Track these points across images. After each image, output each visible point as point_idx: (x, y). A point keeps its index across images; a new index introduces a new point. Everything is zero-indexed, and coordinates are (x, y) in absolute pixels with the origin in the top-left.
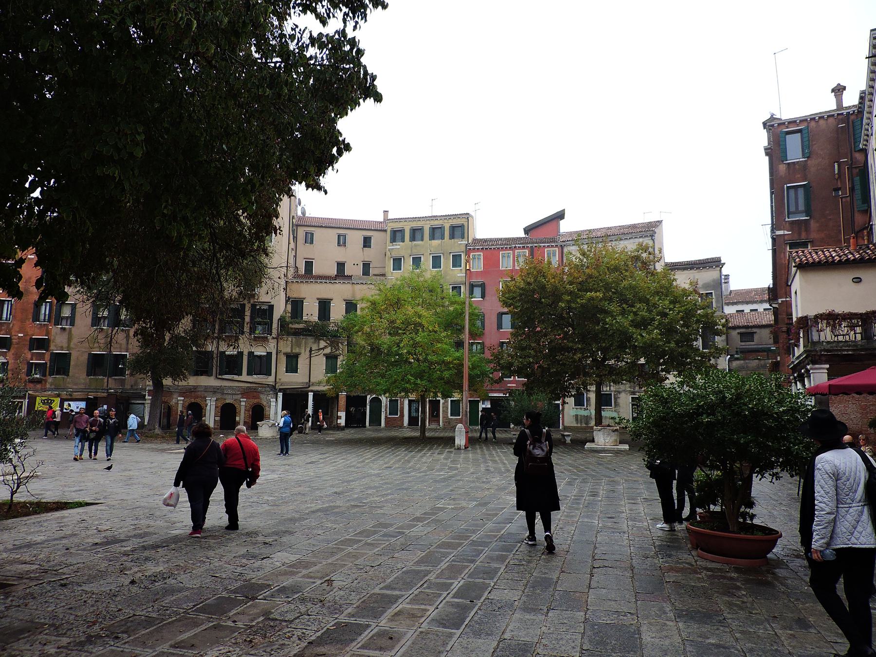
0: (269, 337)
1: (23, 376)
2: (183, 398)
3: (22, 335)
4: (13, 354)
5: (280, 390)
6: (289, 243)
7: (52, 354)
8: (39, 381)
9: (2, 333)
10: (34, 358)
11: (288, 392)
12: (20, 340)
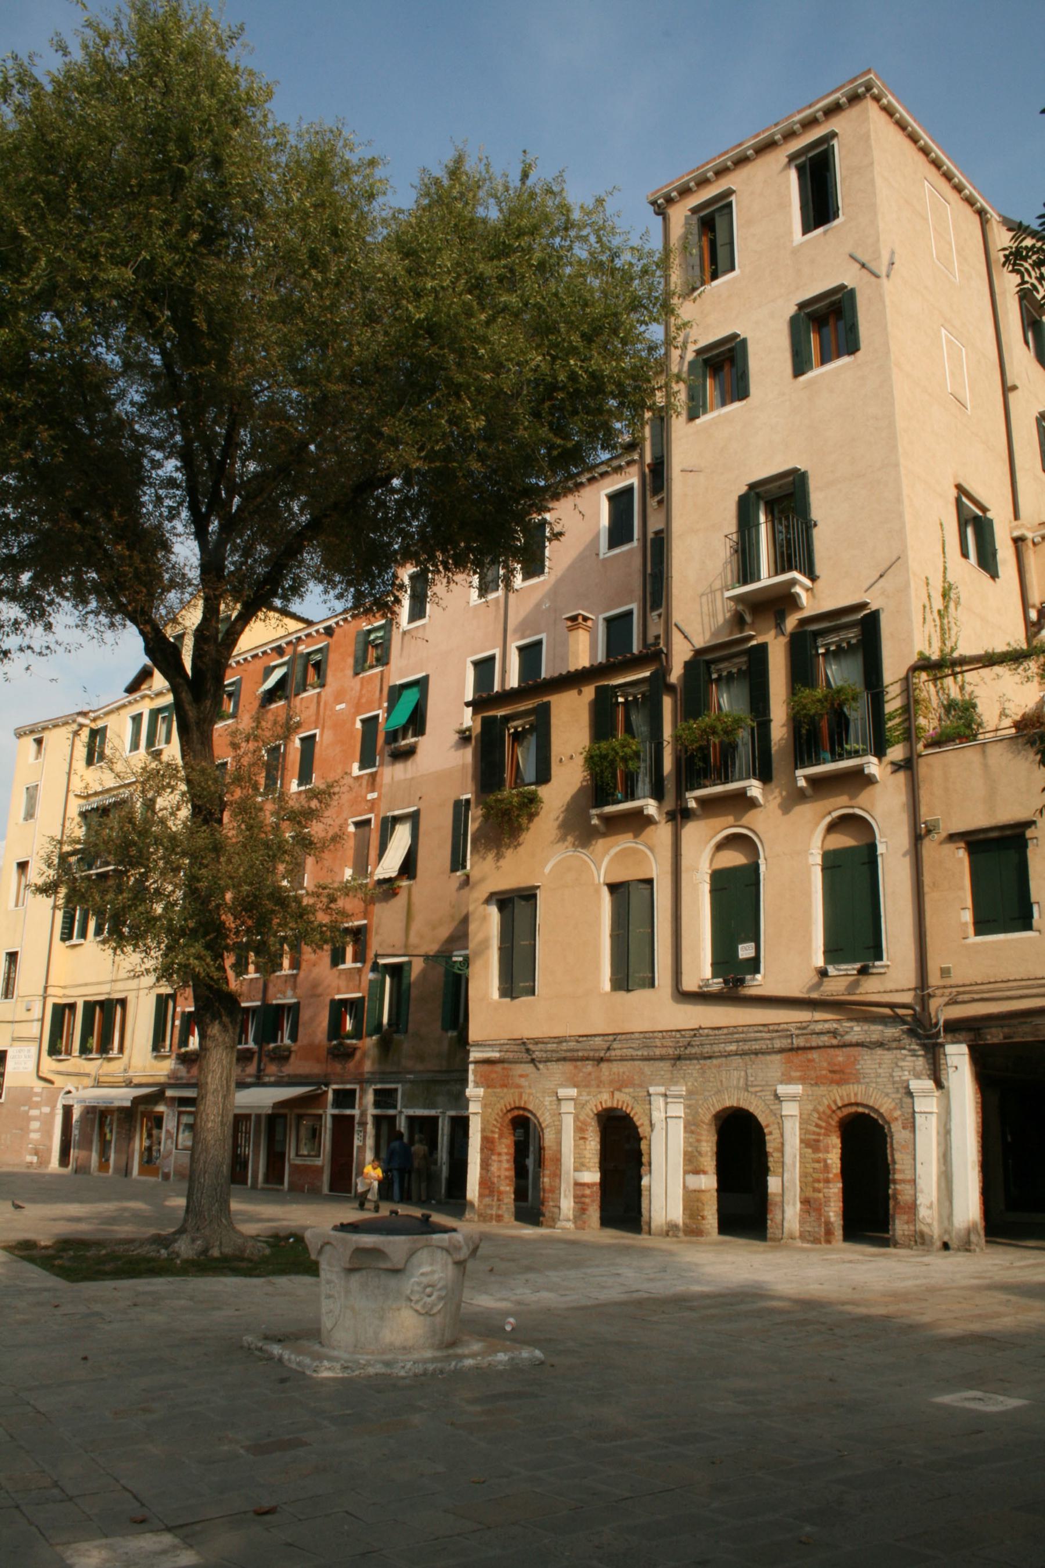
0: (873, 766)
2: (573, 1092)
5: (955, 1028)
6: (1007, 390)
11: (994, 1036)
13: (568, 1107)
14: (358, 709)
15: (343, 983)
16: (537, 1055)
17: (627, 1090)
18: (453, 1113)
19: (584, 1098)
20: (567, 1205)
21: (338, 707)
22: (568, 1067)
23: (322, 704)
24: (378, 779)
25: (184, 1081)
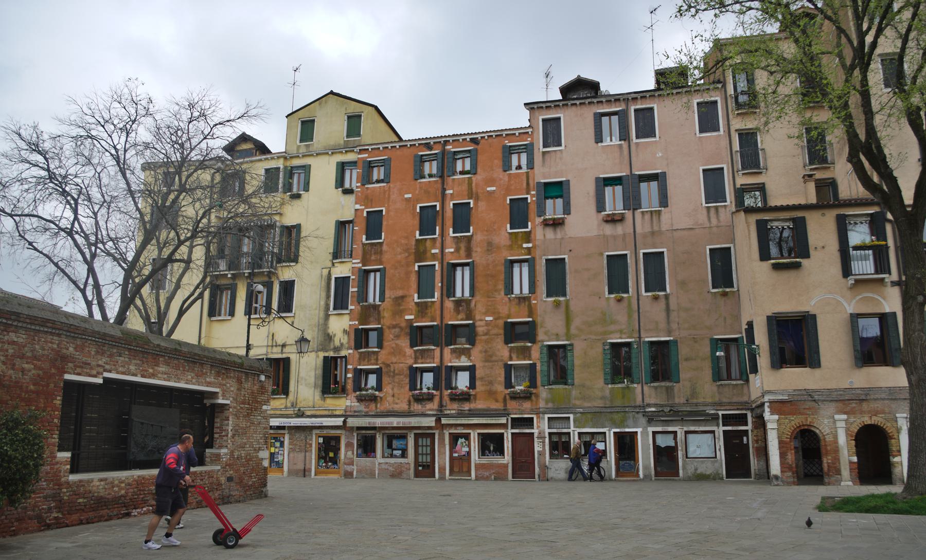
1: (500, 388)
2: (845, 417)
3: (491, 318)
4: (481, 352)
7: (543, 346)
8: (526, 396)
9: (460, 317)
10: (514, 356)
12: (490, 328)
13: (841, 425)
14: (508, 191)
15: (514, 356)
16: (816, 397)
17: (880, 415)
18: (617, 430)
19: (852, 420)
20: (845, 472)
21: (489, 189)
22: (840, 405)
23: (474, 185)
24: (532, 235)
25: (364, 414)
